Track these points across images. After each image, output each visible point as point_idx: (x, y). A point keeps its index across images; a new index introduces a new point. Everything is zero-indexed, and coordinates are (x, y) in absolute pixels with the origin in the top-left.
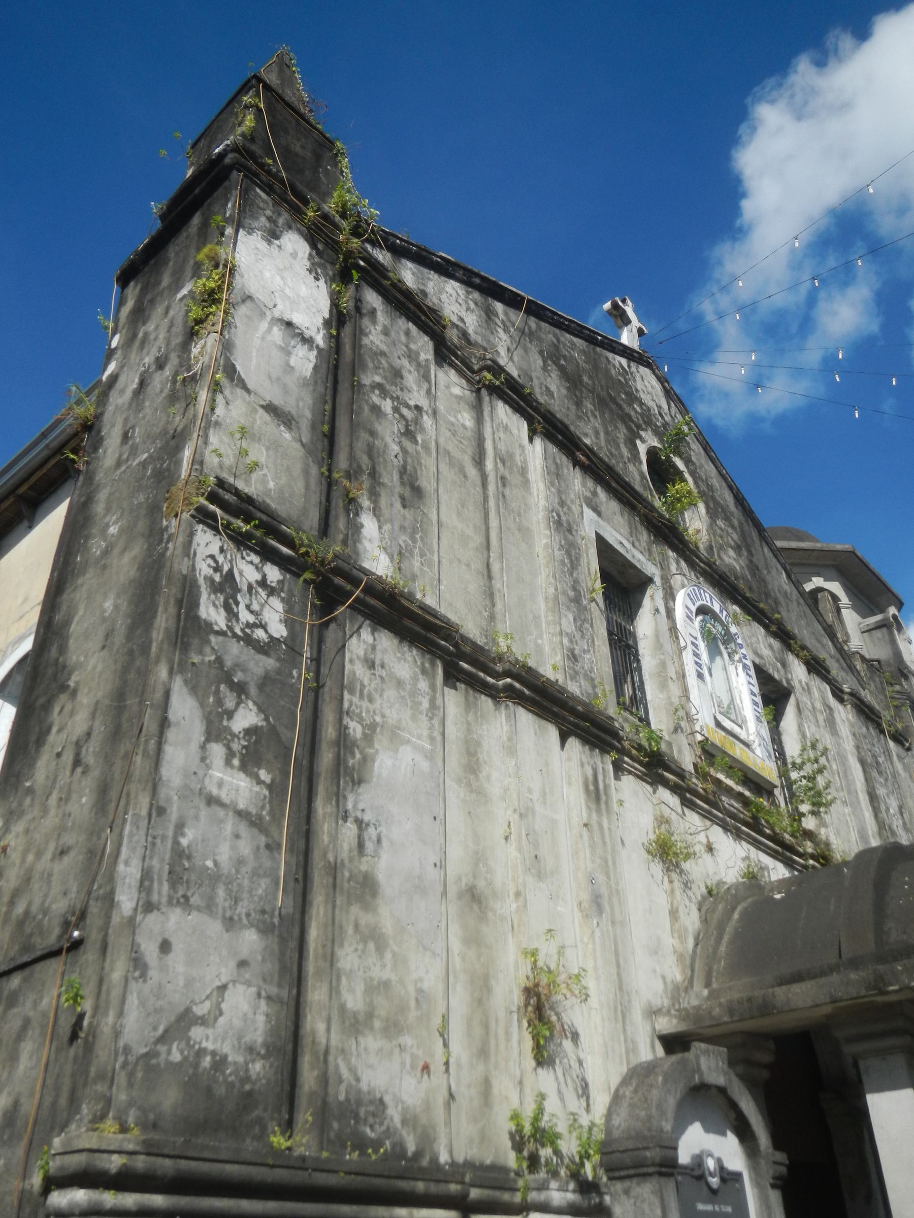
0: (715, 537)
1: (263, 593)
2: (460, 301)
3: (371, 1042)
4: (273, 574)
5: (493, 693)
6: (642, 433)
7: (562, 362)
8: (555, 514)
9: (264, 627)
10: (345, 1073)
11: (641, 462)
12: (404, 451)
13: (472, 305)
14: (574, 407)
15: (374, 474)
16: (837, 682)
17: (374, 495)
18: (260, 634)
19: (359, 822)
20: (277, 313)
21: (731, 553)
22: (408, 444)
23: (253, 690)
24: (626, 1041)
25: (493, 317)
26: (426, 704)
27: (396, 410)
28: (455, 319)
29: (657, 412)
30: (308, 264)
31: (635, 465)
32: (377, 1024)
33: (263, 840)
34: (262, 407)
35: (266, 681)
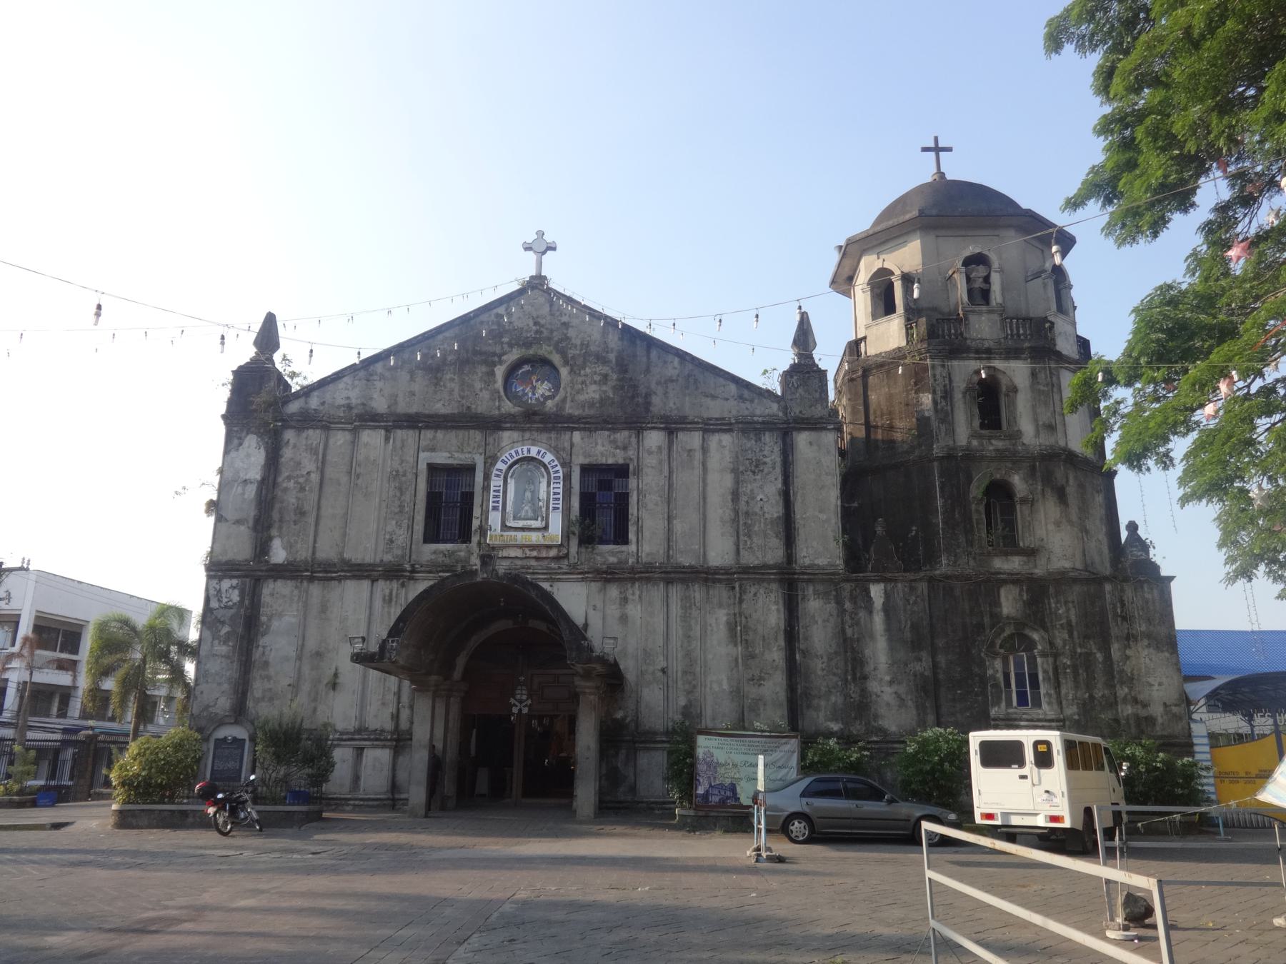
0: (572, 388)
1: (231, 590)
2: (348, 387)
3: (263, 704)
4: (235, 582)
5: (340, 579)
6: (504, 358)
7: (430, 362)
8: (394, 473)
9: (231, 601)
10: (254, 712)
11: (495, 382)
12: (298, 499)
13: (357, 382)
14: (433, 388)
15: (281, 520)
16: (723, 419)
17: (280, 528)
18: (230, 603)
19: (264, 647)
20: (239, 481)
21: (594, 387)
22: (301, 495)
23: (227, 621)
24: (384, 688)
25: (372, 378)
26: (296, 599)
27: (297, 482)
28: (343, 402)
29: (531, 324)
30: (255, 446)
31: (487, 389)
32: (266, 699)
33: (229, 661)
34: (234, 524)
35: (232, 618)
